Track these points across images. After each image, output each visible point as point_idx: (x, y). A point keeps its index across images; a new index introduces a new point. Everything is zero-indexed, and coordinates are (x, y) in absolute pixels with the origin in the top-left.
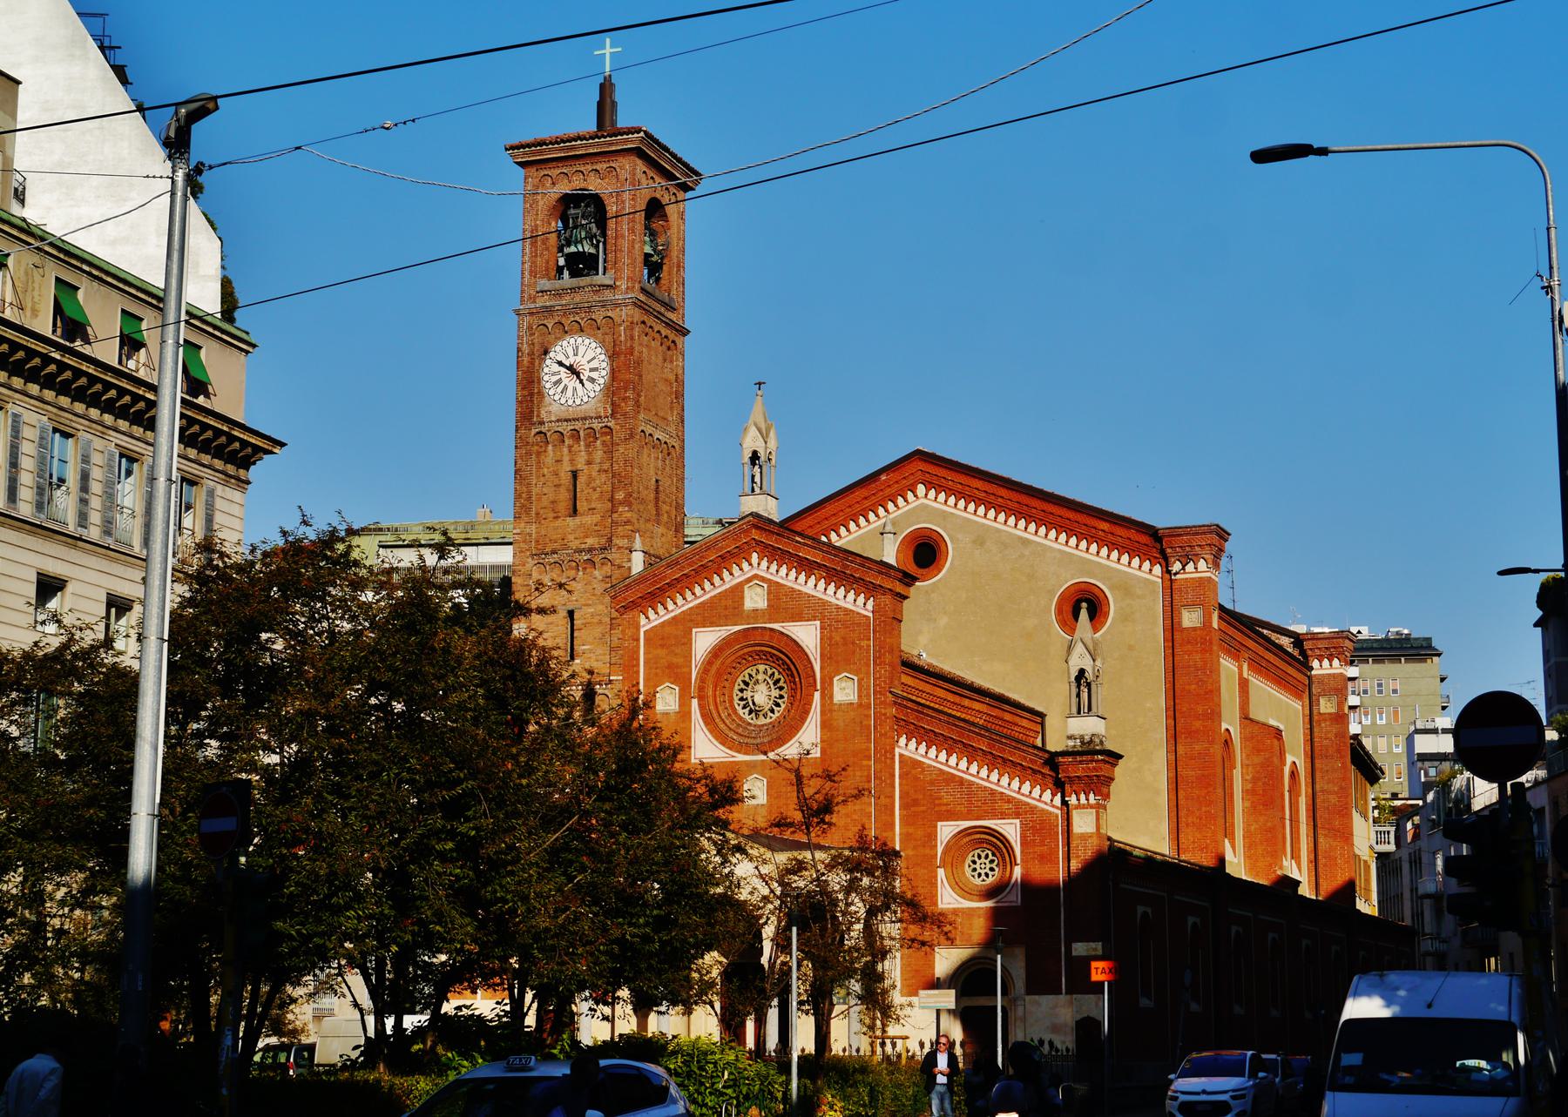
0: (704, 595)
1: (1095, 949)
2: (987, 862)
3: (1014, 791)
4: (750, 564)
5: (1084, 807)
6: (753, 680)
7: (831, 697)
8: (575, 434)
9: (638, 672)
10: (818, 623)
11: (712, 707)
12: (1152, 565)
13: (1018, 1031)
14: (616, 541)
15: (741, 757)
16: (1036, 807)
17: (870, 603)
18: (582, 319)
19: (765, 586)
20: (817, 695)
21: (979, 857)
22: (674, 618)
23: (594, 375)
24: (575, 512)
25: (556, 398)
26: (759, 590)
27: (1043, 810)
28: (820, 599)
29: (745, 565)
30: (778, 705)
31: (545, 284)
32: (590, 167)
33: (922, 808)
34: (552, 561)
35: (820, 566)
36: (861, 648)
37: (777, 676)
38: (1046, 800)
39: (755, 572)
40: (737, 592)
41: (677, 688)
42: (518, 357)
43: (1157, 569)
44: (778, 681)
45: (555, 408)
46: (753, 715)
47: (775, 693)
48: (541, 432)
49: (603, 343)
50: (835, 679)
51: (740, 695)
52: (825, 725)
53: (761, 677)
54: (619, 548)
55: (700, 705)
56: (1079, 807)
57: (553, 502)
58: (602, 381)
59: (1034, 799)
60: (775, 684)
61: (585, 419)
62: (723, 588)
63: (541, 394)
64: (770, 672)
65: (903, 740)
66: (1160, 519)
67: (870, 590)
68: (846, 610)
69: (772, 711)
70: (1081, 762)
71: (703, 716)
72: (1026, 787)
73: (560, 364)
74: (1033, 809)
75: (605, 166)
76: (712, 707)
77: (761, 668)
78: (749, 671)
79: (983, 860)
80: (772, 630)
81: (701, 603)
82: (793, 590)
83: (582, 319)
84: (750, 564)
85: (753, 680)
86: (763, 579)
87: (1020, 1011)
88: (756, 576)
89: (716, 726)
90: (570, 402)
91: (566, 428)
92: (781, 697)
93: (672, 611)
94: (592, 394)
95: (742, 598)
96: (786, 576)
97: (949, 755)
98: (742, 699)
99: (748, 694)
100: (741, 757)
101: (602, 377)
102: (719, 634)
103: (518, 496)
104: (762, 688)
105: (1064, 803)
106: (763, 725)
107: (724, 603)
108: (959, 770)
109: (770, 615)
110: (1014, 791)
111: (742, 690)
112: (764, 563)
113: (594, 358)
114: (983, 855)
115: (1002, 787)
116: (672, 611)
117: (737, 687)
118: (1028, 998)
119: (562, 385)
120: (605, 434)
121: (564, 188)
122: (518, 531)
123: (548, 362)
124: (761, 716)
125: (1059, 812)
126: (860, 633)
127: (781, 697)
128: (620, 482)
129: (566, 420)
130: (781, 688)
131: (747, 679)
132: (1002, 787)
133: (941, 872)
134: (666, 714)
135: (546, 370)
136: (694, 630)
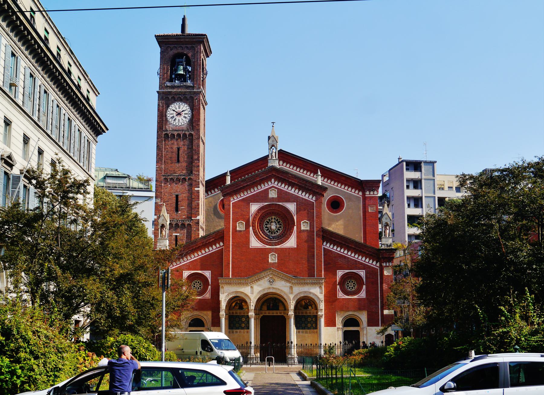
0: (254, 192)
1: (392, 312)
2: (352, 283)
3: (363, 261)
4: (272, 183)
5: (388, 267)
7: (301, 227)
8: (179, 135)
9: (230, 216)
10: (295, 203)
11: (257, 229)
12: (359, 192)
13: (364, 338)
14: (194, 172)
15: (268, 247)
16: (371, 266)
17: (314, 198)
18: (182, 96)
19: (276, 190)
20: (295, 227)
21: (196, 282)
22: (243, 199)
23: (186, 116)
24: (178, 161)
25: (172, 122)
26: (274, 191)
27: (373, 267)
28: (296, 195)
29: (270, 183)
31: (169, 84)
32: (185, 46)
33: (332, 266)
34: (171, 178)
35: (297, 185)
36: (311, 212)
38: (374, 264)
39: (273, 185)
40: (266, 192)
41: (244, 223)
42: (158, 107)
43: (361, 193)
45: (171, 126)
46: (270, 233)
47: (278, 226)
48: (166, 134)
49: (189, 105)
51: (266, 226)
52: (298, 237)
53: (273, 220)
54: (195, 175)
55: (253, 229)
56: (386, 266)
57: (170, 158)
58: (189, 118)
59: (370, 264)
60: (278, 223)
61: (183, 130)
62: (261, 190)
63: (167, 120)
64: (276, 219)
65: (325, 244)
66: (362, 177)
67: (314, 193)
68: (305, 199)
69: (277, 232)
70: (388, 252)
71: (253, 232)
72: (367, 260)
73: (174, 110)
74: (370, 266)
75: (190, 46)
76: (257, 229)
77: (273, 217)
78: (269, 218)
79: (351, 283)
80: (278, 204)
81: (253, 195)
83: (182, 96)
87: (365, 332)
88: (273, 187)
90: (177, 124)
91: (176, 133)
92: (280, 227)
93: (243, 197)
94: (185, 122)
95: (268, 193)
96: (284, 187)
97: (341, 249)
98: (266, 227)
99: (269, 226)
100: (268, 247)
101: (188, 117)
102: (260, 205)
103: (158, 155)
104: (274, 224)
105: (381, 265)
106: (274, 236)
108: (344, 254)
110: (363, 261)
111: (266, 224)
112: (276, 183)
113: (186, 110)
114: (200, 283)
115: (359, 259)
116: (243, 197)
117: (264, 223)
118: (368, 328)
119: (174, 118)
120: (190, 136)
121: (175, 51)
122: (158, 167)
123: (169, 110)
125: (378, 268)
127: (280, 227)
128: (196, 152)
129: (176, 131)
130: (280, 224)
131: (268, 221)
132: (359, 259)
133: (338, 287)
134: (240, 231)
135: (168, 112)
136: (251, 203)
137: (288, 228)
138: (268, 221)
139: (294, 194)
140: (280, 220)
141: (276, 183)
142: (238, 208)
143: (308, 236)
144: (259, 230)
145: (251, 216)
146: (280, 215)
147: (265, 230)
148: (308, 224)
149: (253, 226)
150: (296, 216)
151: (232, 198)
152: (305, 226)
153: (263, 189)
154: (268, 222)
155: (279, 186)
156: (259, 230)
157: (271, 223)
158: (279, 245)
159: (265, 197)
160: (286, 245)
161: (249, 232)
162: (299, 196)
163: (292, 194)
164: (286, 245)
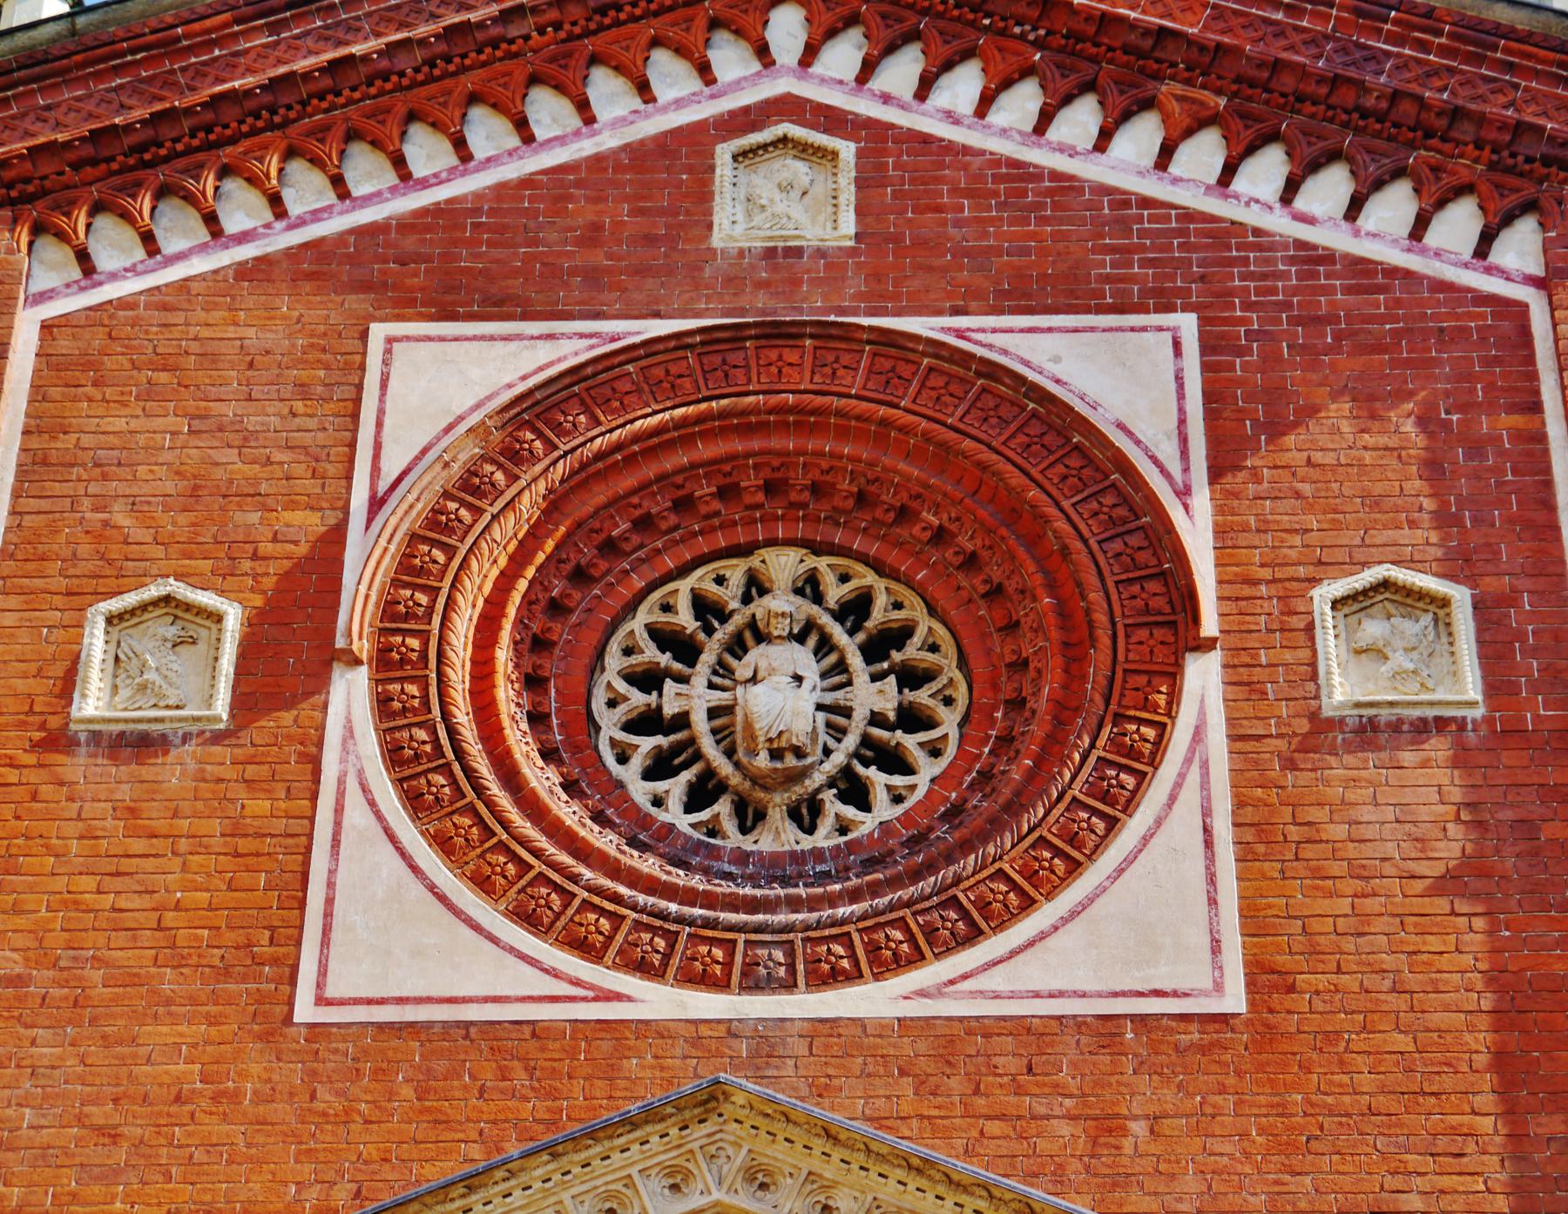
4: (763, 52)
6: (723, 633)
11: (463, 717)
19: (847, 150)
26: (798, 170)
28: (1188, 215)
30: (895, 762)
36: (1476, 448)
37: (879, 614)
41: (234, 617)
44: (901, 635)
46: (723, 807)
50: (1325, 593)
51: (639, 699)
53: (781, 604)
55: (382, 705)
60: (874, 650)
62: (586, 147)
64: (835, 593)
69: (856, 794)
71: (394, 756)
77: (783, 565)
78: (700, 578)
82: (1020, 172)
84: (763, 52)
85: (723, 633)
86: (832, 120)
88: (788, 107)
89: (487, 822)
92: (912, 719)
93: (243, 237)
95: (703, 195)
98: (646, 723)
107: (581, 212)
109: (876, 276)
111: (648, 680)
116: (243, 237)
117: (614, 661)
124: (777, 815)
126: (1464, 376)
130: (911, 678)
131: (685, 618)
136: (378, 332)
137: (1064, 712)
138: (685, 618)
139: (1146, 202)
140: (916, 610)
141: (844, 55)
142: (149, 393)
143: (1475, 814)
144: (503, 655)
145: (376, 504)
146: (904, 514)
147: (630, 775)
148: (1444, 624)
149: (386, 664)
150: (1202, 499)
151: (50, 249)
152: (1400, 660)
153: (607, 141)
154: (686, 650)
155: (886, 98)
156: (503, 655)
157: (737, 647)
158: (886, 964)
159: (650, 240)
160: (1031, 972)
161: (314, 764)
162: (1252, 217)
163: (1121, 199)
164: (1031, 972)
